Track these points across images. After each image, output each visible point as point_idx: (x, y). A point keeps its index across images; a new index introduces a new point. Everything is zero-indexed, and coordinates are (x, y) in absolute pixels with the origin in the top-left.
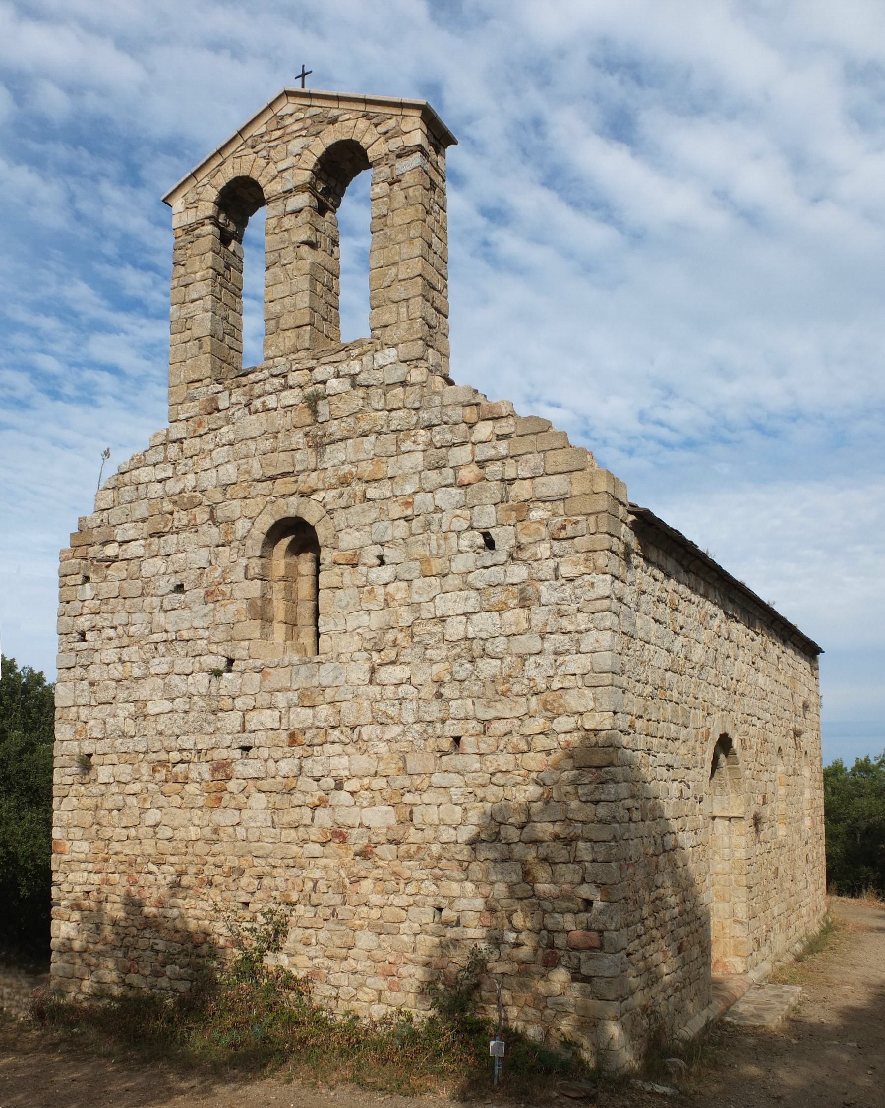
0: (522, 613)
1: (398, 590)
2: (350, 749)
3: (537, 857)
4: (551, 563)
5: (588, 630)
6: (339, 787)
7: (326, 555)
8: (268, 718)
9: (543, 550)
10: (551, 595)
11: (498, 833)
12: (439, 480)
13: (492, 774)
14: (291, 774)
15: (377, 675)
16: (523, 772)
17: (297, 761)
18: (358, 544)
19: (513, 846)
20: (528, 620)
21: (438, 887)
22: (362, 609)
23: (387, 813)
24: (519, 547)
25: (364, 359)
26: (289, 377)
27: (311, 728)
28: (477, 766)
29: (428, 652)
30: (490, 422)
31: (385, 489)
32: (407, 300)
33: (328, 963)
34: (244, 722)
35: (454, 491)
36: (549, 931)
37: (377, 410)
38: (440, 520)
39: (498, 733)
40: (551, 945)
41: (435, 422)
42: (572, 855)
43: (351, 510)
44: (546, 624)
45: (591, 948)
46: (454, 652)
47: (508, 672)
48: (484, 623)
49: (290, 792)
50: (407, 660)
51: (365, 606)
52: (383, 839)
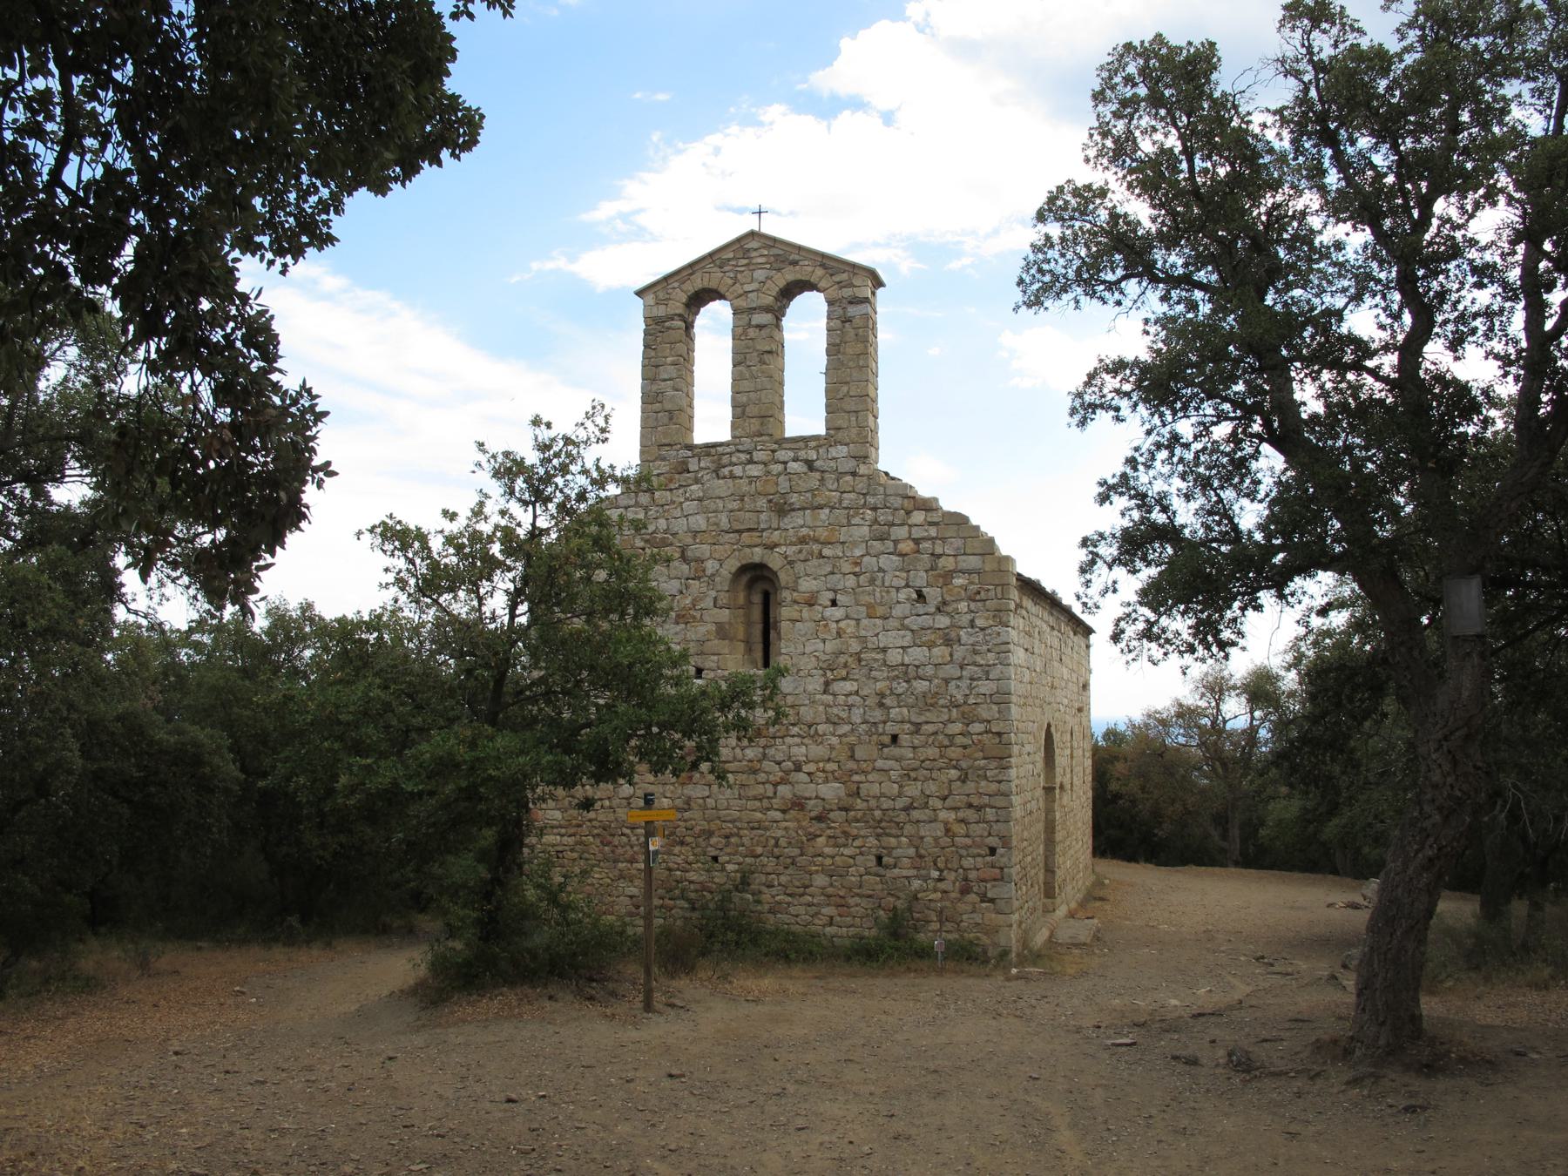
0: (945, 650)
2: (806, 741)
4: (969, 617)
6: (798, 768)
7: (786, 595)
9: (963, 606)
24: (945, 603)
35: (894, 558)
40: (966, 879)
48: (918, 654)
49: (755, 772)
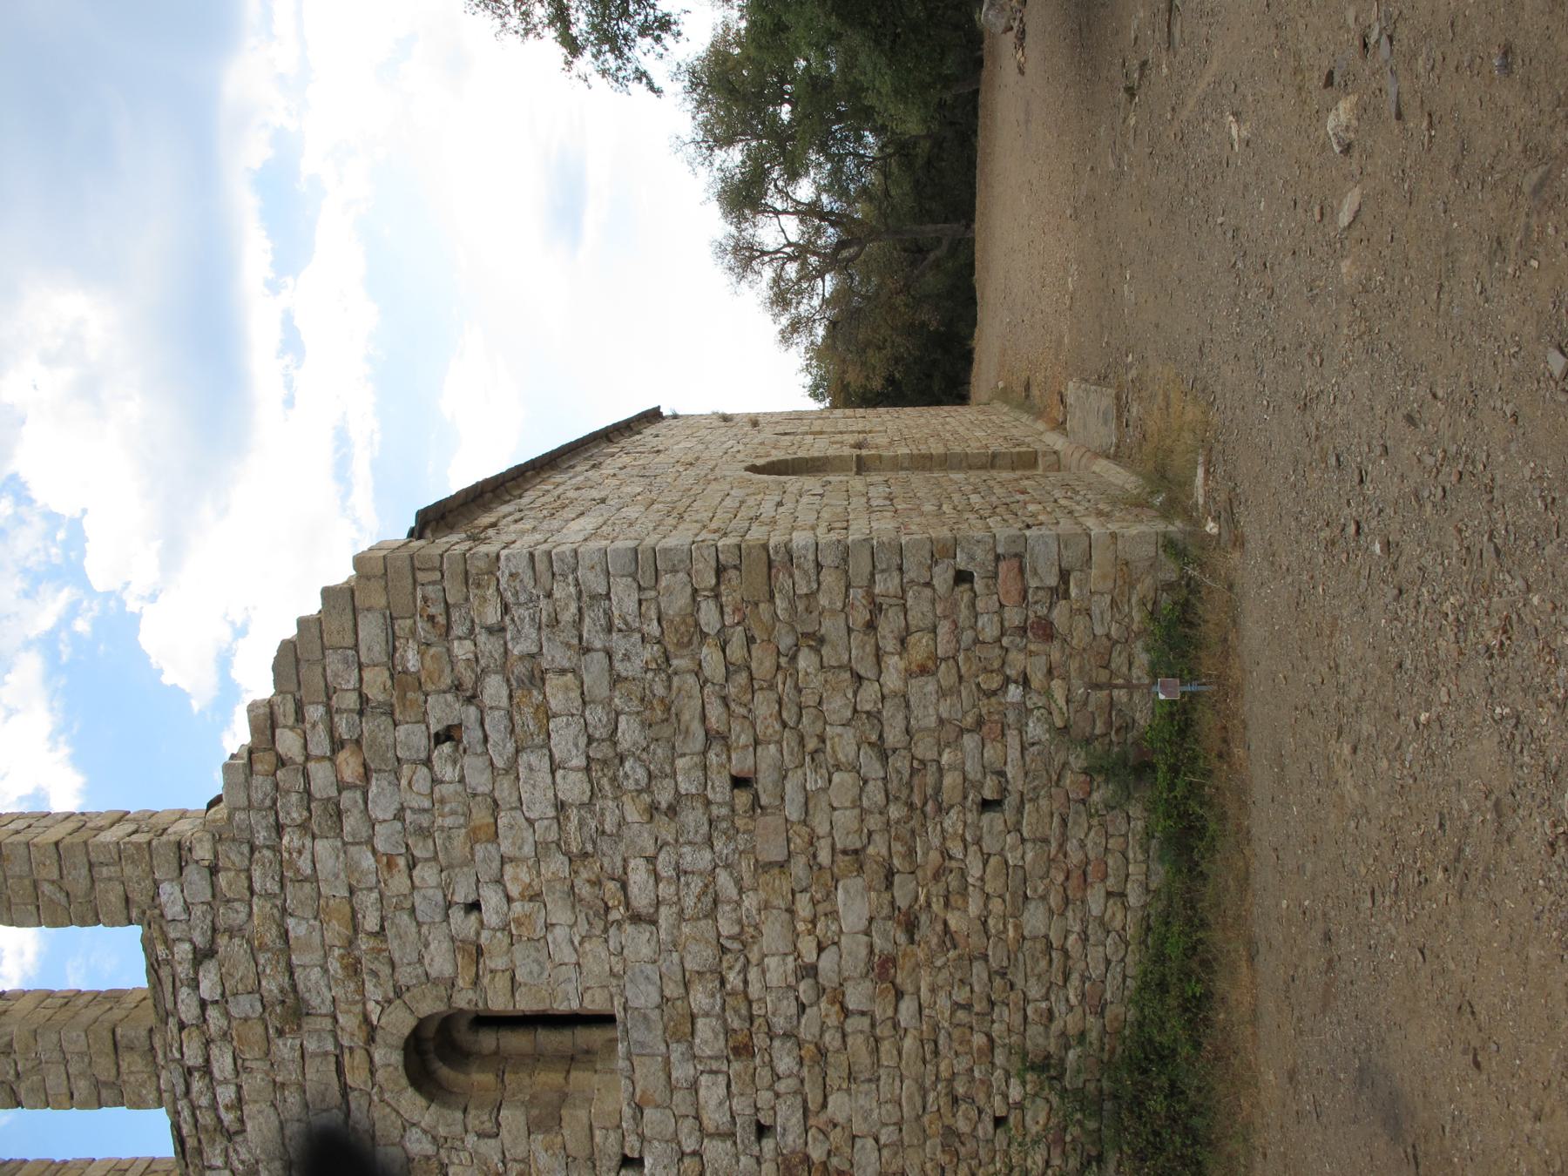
0: (553, 681)
1: (516, 879)
2: (754, 957)
3: (900, 654)
4: (482, 637)
5: (577, 584)
6: (811, 971)
7: (464, 999)
8: (711, 1092)
9: (462, 650)
10: (527, 637)
11: (868, 713)
12: (356, 812)
13: (784, 725)
14: (796, 1052)
15: (644, 911)
16: (780, 678)
17: (777, 1043)
18: (446, 945)
19: (886, 691)
20: (563, 672)
21: (952, 806)
22: (545, 937)
23: (847, 891)
24: (457, 687)
25: (172, 935)
26: (190, 1063)
27: (725, 1021)
28: (772, 748)
29: (608, 828)
30: (278, 732)
31: (368, 900)
32: (91, 865)
33: (1075, 979)
34: (719, 1135)
35: (373, 790)
36: (1002, 634)
37: (250, 914)
38: (413, 810)
39: (725, 716)
40: (1022, 630)
41: (272, 820)
42: (894, 601)
43: (396, 956)
44: (568, 646)
45: (1022, 570)
46: (607, 787)
47: (636, 702)
48: (565, 739)
49: (822, 1052)
50: (619, 863)
51: (540, 933)
52: (886, 896)
